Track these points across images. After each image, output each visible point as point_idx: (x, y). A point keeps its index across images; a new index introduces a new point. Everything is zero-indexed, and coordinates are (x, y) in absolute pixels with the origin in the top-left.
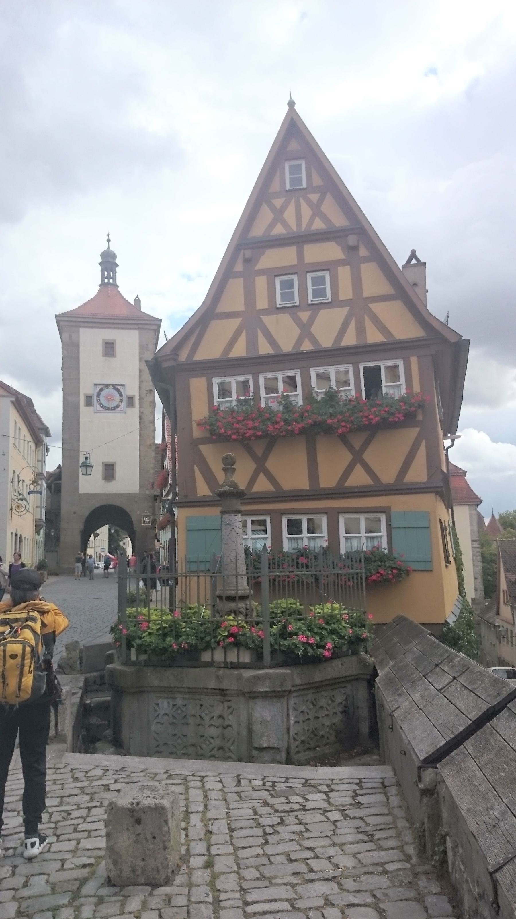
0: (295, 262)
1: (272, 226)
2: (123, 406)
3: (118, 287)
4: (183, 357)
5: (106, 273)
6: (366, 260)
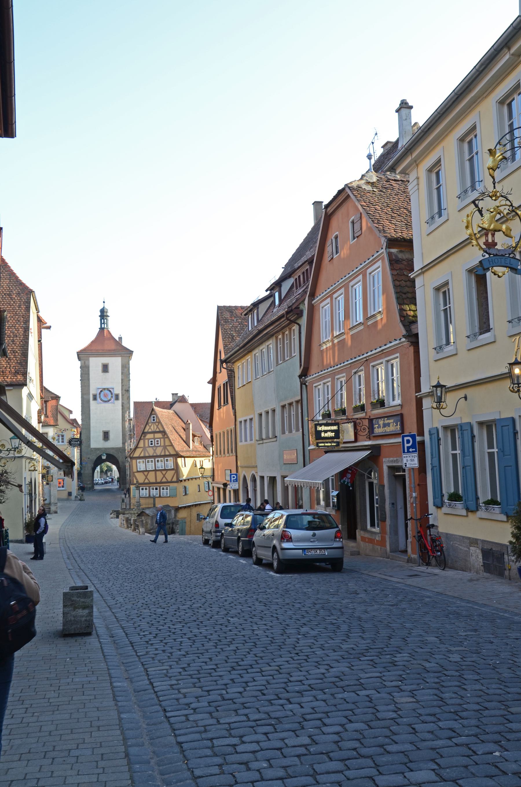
4: (131, 456)
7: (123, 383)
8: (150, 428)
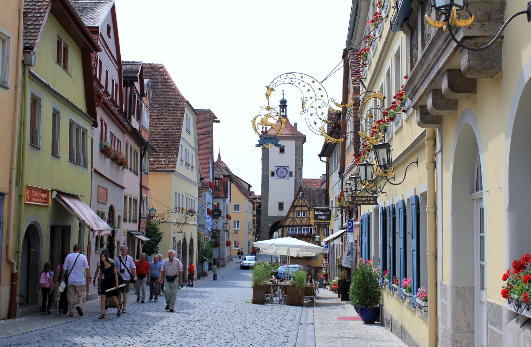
0: (300, 210)
1: (297, 204)
2: (287, 176)
3: (287, 116)
4: (283, 224)
5: (282, 109)
7: (297, 162)
8: (298, 202)
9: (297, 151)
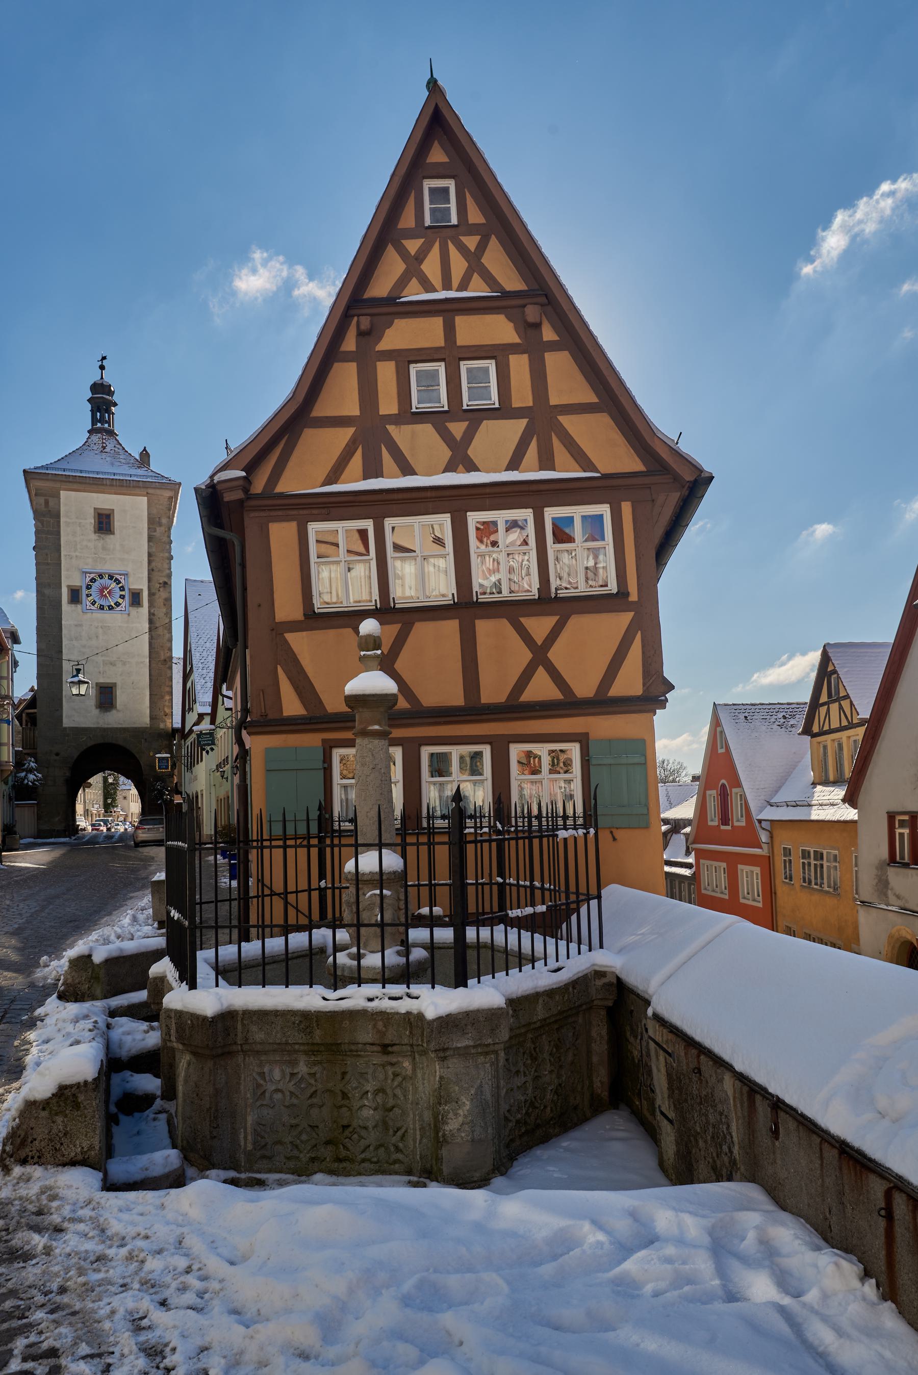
0: (442, 344)
1: (402, 282)
2: (125, 603)
3: (117, 435)
5: (98, 414)
6: (553, 346)
7: (153, 564)
9: (155, 531)
